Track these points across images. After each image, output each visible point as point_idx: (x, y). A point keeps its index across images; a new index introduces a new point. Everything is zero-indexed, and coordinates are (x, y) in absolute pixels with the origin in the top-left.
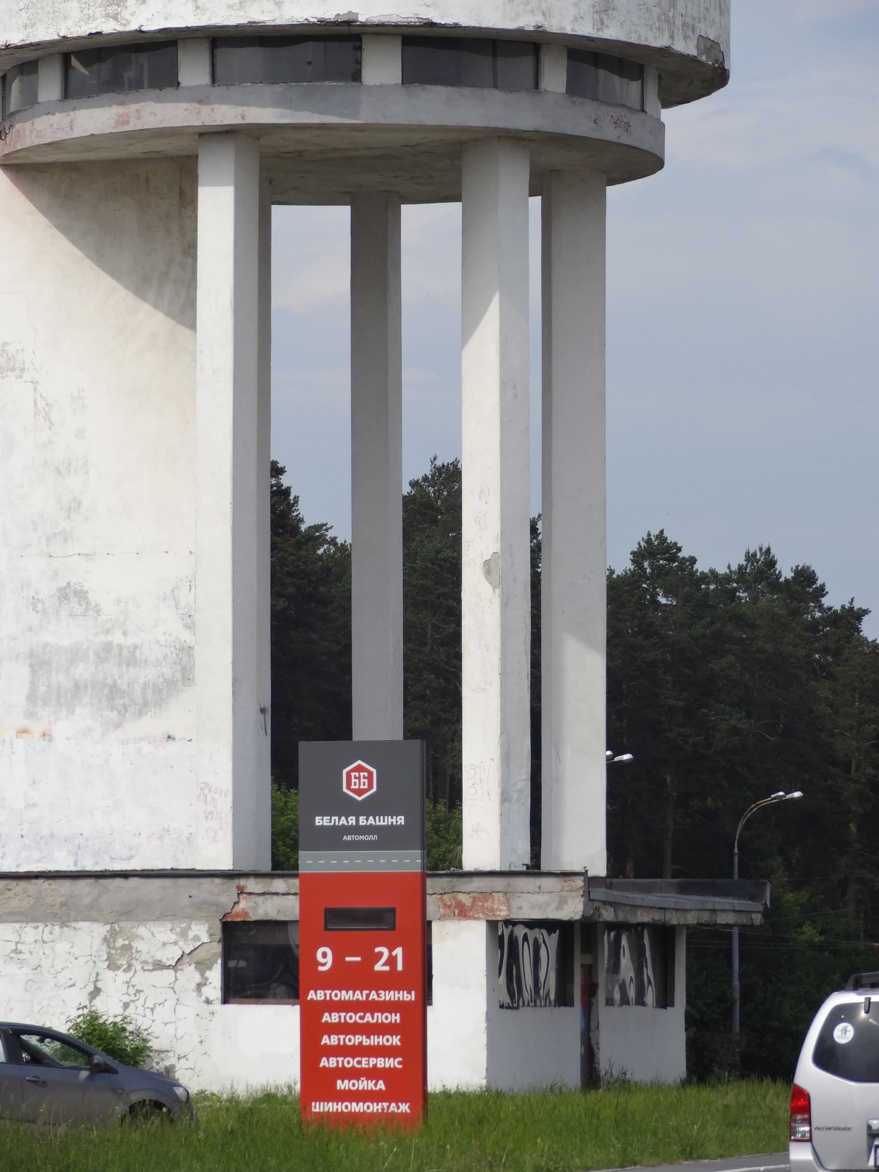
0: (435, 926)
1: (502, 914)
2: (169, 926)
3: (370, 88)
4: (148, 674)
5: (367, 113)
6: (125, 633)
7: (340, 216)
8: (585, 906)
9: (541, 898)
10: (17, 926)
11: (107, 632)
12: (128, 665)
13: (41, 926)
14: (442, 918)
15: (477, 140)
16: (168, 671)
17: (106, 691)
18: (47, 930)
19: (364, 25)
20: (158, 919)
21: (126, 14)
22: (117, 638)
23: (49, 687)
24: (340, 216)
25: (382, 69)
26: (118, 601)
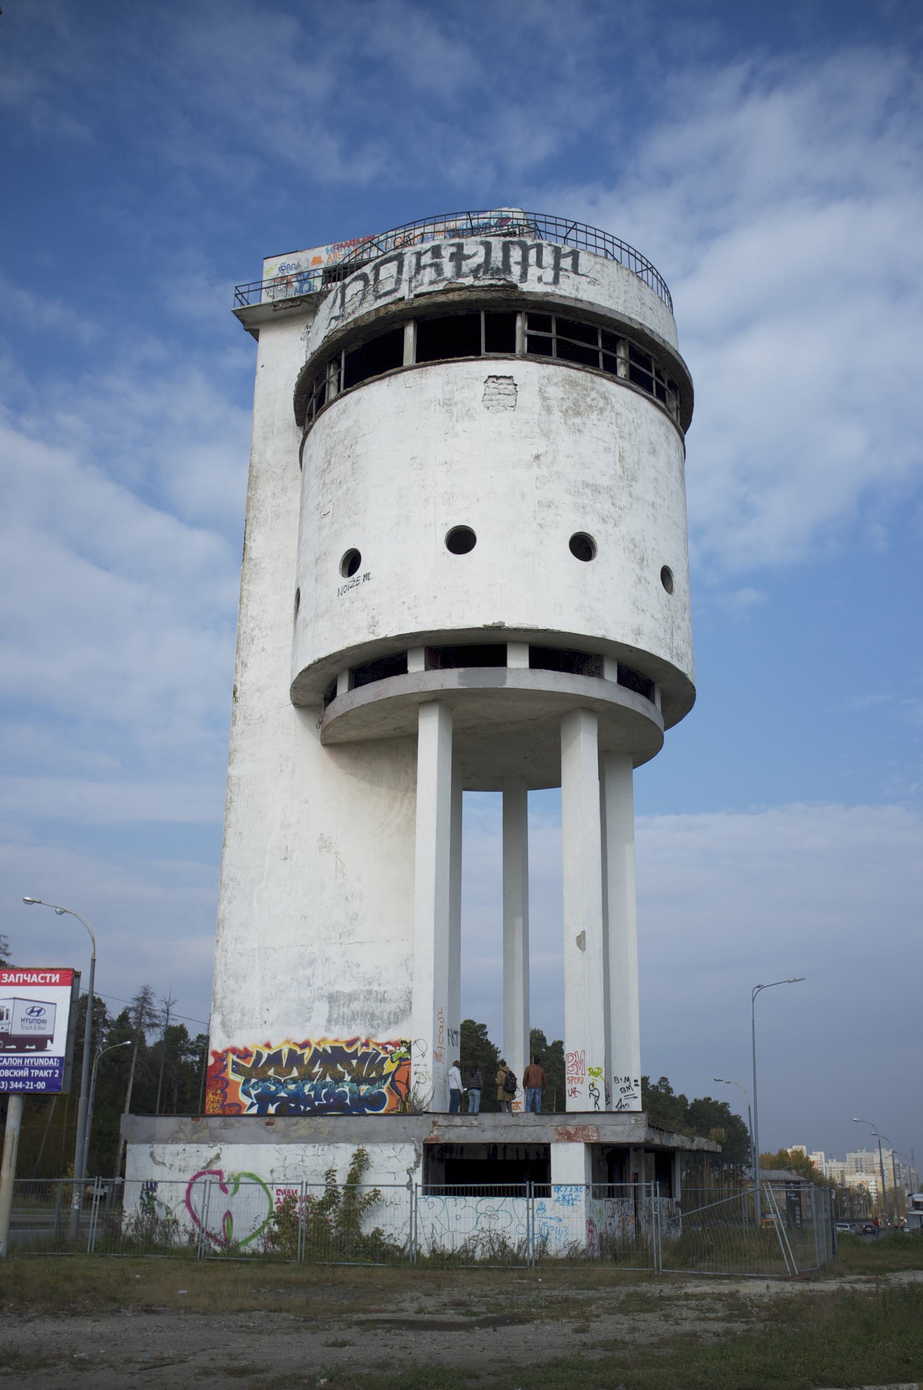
0: (553, 1147)
1: (594, 1138)
2: (392, 1146)
3: (511, 669)
4: (391, 1007)
5: (511, 683)
6: (379, 985)
7: (496, 799)
8: (647, 1133)
9: (619, 1129)
10: (303, 1145)
11: (370, 983)
12: (381, 1001)
13: (317, 1145)
14: (557, 1141)
15: (569, 712)
16: (402, 1005)
17: (368, 1017)
18: (320, 1148)
19: (508, 629)
20: (386, 1142)
21: (378, 630)
22: (375, 987)
23: (339, 1015)
24: (496, 799)
25: (518, 660)
26: (376, 967)
